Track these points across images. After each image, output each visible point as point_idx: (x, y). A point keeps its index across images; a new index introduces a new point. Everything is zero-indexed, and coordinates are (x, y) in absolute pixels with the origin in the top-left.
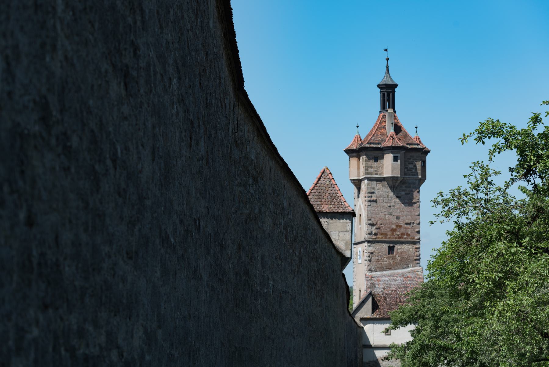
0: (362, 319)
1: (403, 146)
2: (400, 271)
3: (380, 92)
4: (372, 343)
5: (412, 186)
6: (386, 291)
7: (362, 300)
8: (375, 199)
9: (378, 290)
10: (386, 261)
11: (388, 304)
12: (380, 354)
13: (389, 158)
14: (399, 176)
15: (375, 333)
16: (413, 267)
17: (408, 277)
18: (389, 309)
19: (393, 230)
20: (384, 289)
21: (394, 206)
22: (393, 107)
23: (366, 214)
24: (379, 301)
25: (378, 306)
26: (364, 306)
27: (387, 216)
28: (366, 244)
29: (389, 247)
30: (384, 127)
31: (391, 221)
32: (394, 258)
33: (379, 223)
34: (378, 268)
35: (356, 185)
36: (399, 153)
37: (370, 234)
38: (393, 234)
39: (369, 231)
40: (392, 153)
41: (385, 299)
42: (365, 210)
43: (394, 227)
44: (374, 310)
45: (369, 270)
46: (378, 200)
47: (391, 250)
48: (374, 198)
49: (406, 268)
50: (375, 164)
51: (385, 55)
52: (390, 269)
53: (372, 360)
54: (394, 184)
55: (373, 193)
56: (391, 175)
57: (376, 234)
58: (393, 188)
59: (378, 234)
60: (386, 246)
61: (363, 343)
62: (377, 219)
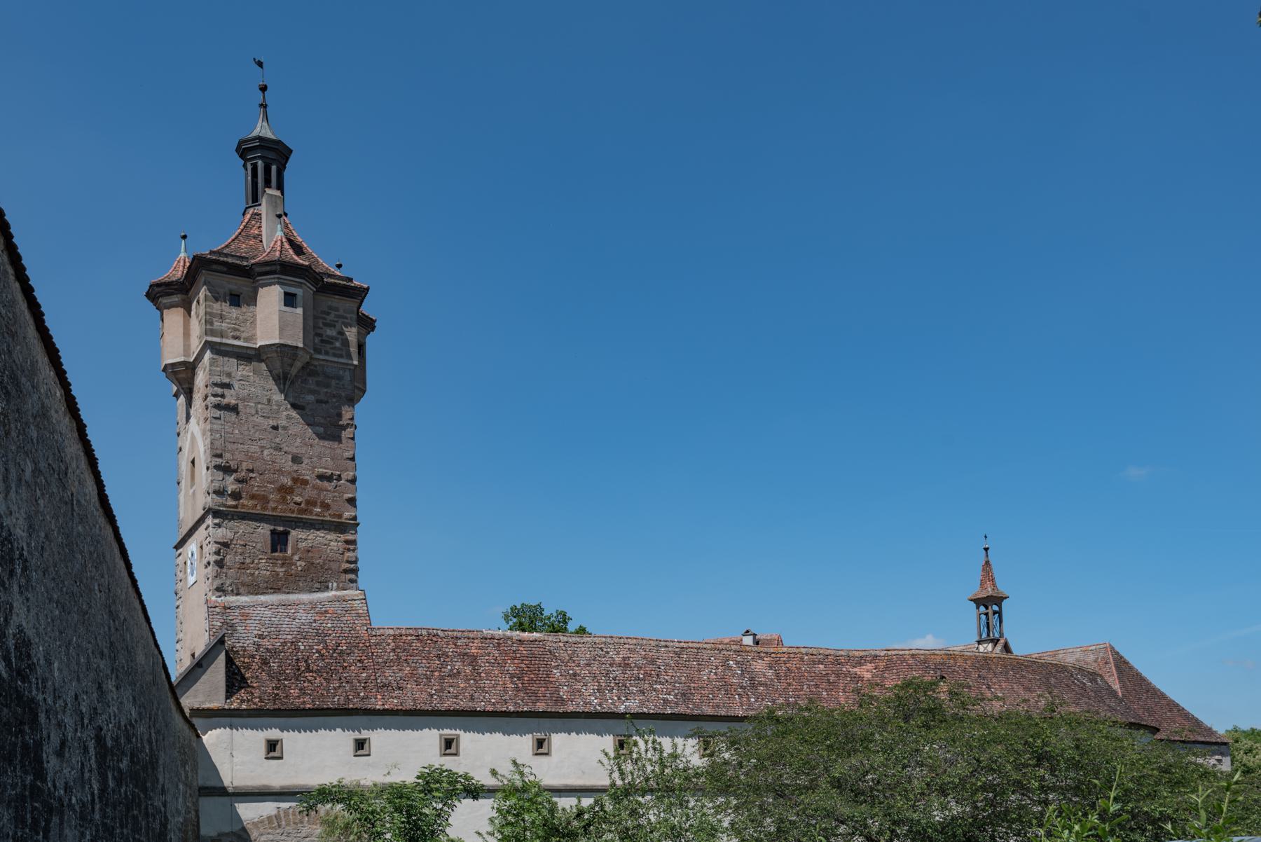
0: (198, 712)
1: (310, 266)
2: (305, 597)
3: (245, 166)
4: (227, 782)
5: (333, 382)
6: (266, 643)
7: (196, 661)
8: (233, 402)
9: (245, 638)
10: (264, 569)
11: (277, 676)
12: (249, 812)
13: (270, 297)
14: (301, 345)
15: (235, 754)
16: (338, 589)
17: (326, 612)
18: (278, 688)
19: (284, 491)
20: (261, 636)
21: (285, 428)
22: (280, 187)
23: (209, 440)
24: (248, 667)
25: (244, 679)
26: (204, 677)
27: (266, 452)
28: (210, 521)
29: (273, 532)
30: (258, 237)
31: (277, 466)
32: (287, 562)
33: (244, 466)
34: (243, 584)
35: (179, 382)
36: (300, 285)
37: (220, 493)
38: (284, 499)
39: (217, 485)
40: (279, 283)
41: (265, 662)
42: (204, 434)
43: (287, 481)
44: (231, 690)
45: (218, 589)
46: (240, 407)
47: (279, 541)
48: (230, 399)
49: (319, 590)
50: (234, 312)
51: (257, 77)
52: (277, 590)
53: (227, 829)
54: (285, 367)
55: (228, 386)
56: (277, 341)
57: (236, 495)
58: (282, 380)
59: (244, 495)
60: (264, 530)
61: (201, 783)
62: (240, 457)
